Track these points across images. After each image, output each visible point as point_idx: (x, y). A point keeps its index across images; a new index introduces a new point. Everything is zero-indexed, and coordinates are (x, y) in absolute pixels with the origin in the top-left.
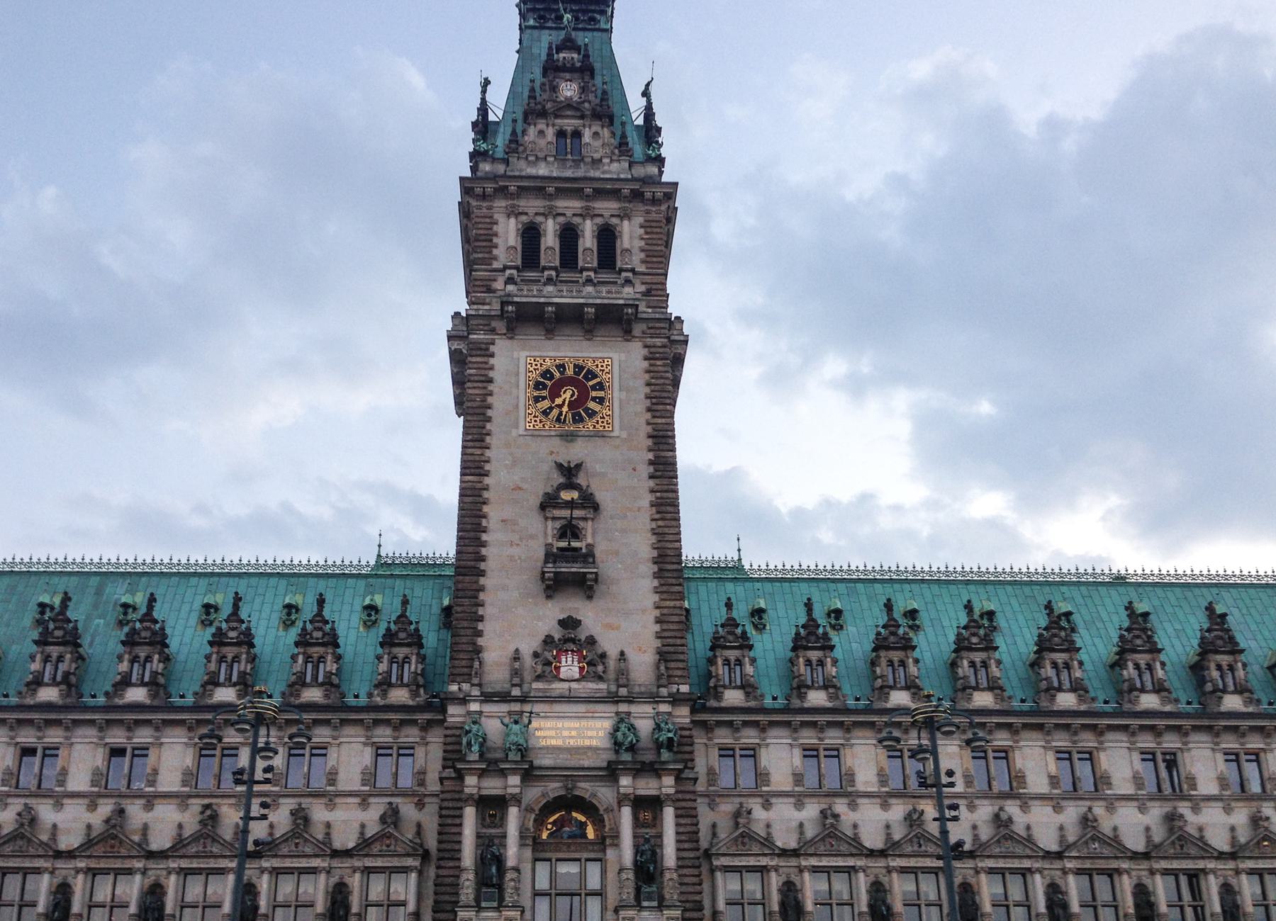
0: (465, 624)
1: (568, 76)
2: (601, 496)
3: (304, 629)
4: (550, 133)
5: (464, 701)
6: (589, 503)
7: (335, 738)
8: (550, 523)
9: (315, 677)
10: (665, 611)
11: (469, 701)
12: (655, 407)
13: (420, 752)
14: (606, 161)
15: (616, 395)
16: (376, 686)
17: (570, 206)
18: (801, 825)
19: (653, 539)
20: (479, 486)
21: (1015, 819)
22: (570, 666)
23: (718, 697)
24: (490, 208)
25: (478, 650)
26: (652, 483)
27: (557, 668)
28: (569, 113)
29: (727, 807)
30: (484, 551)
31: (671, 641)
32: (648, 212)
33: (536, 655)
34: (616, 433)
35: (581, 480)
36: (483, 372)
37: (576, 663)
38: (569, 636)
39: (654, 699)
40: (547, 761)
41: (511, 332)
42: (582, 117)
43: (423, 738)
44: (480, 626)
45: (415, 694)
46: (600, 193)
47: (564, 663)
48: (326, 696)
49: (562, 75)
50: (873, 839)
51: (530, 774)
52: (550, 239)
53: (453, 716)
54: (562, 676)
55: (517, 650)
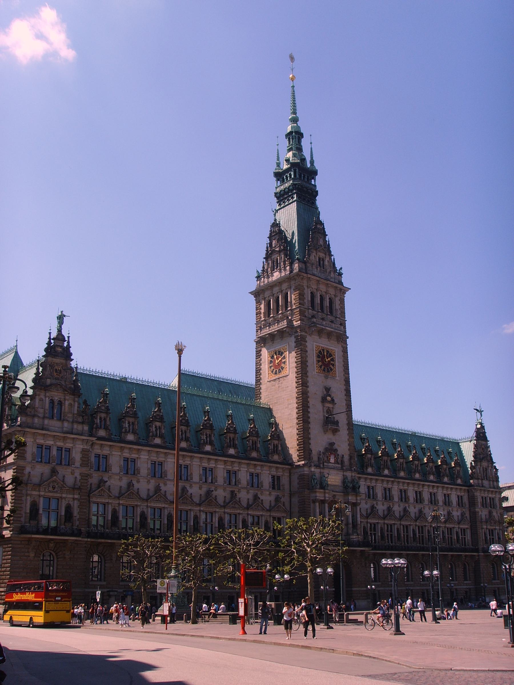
1: (320, 235)
2: (336, 401)
14: (332, 273)
15: (337, 364)
18: (367, 509)
26: (345, 397)
34: (337, 378)
41: (311, 335)
52: (318, 300)
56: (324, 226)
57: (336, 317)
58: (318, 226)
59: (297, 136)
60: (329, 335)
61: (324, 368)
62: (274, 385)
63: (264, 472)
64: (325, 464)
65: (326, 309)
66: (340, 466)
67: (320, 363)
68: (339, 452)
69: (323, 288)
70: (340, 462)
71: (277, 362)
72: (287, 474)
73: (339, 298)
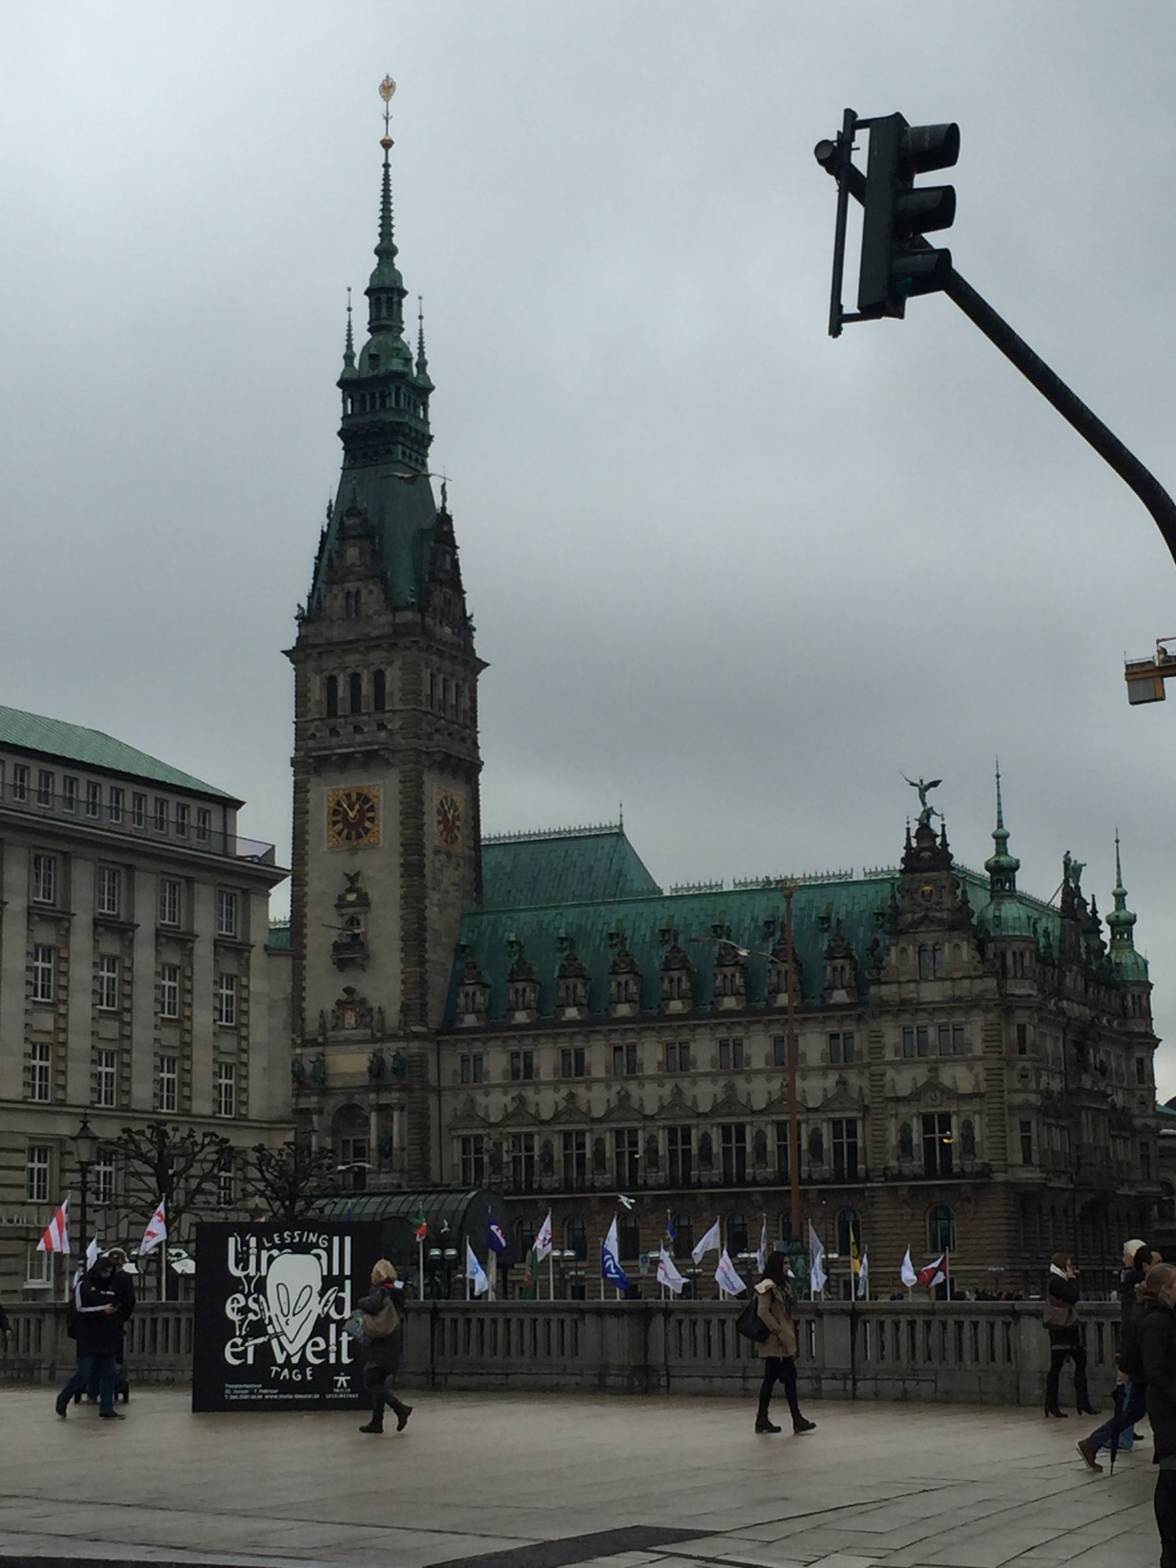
4: (341, 596)
6: (364, 901)
15: (381, 814)
17: (352, 659)
21: (633, 1093)
22: (350, 1018)
23: (462, 1021)
26: (401, 881)
28: (353, 577)
29: (463, 1096)
33: (333, 1011)
35: (358, 885)
38: (351, 1000)
39: (394, 1037)
40: (336, 1083)
44: (304, 994)
46: (369, 649)
50: (546, 1115)
51: (325, 1092)
52: (342, 691)
61: (349, 833)
65: (367, 704)
67: (339, 826)
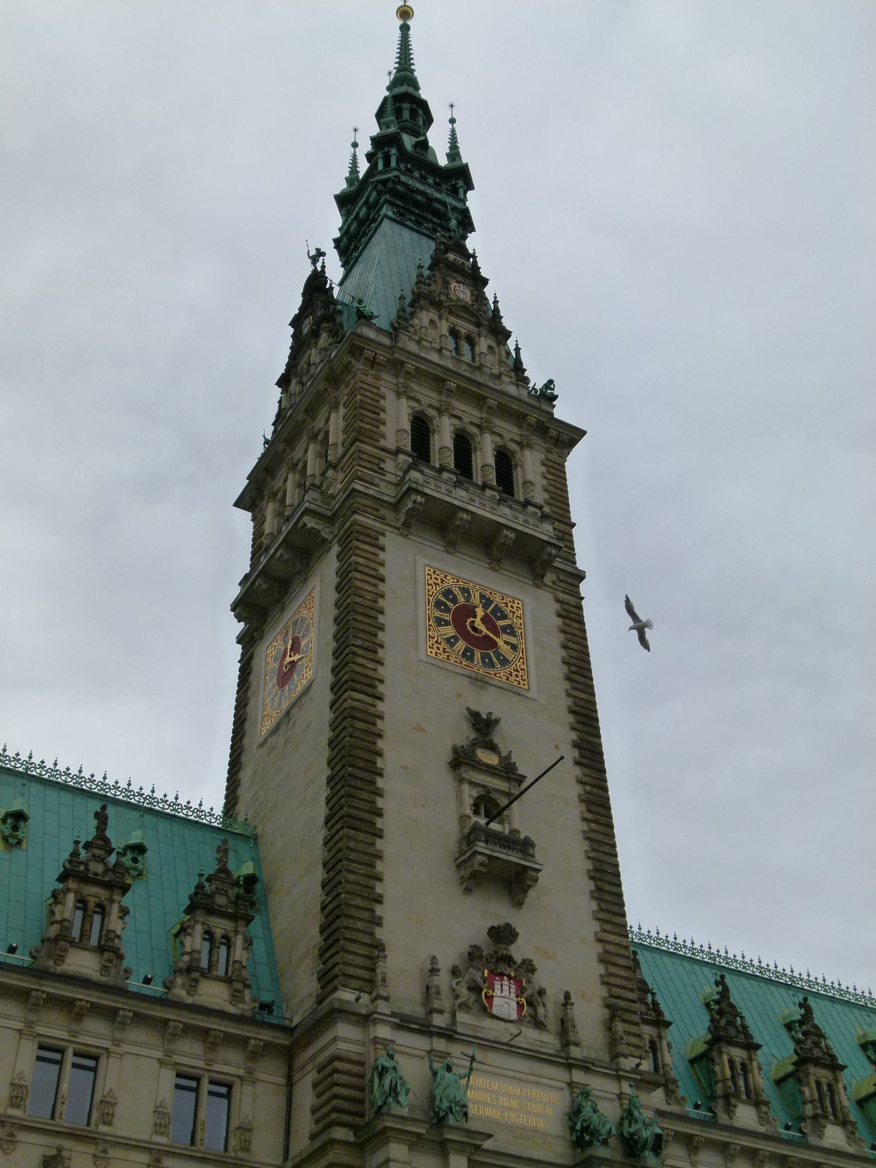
0: (359, 902)
1: (460, 278)
3: (75, 854)
4: (444, 327)
5: (365, 1020)
7: (117, 1042)
8: (466, 787)
9: (84, 933)
10: (610, 948)
11: (375, 1022)
12: (575, 677)
13: (243, 1094)
16: (177, 971)
19: (586, 846)
20: (372, 710)
24: (378, 378)
25: (380, 946)
27: (490, 998)
30: (380, 802)
31: (621, 992)
32: (549, 451)
33: (455, 972)
36: (373, 565)
37: (513, 995)
42: (478, 325)
43: (250, 1071)
44: (379, 910)
45: (236, 997)
47: (497, 992)
48: (104, 969)
49: (454, 274)
53: (346, 1040)
54: (495, 1011)
55: (434, 958)
56: (475, 262)
57: (527, 503)
58: (451, 256)
59: (406, 106)
60: (488, 542)
61: (467, 650)
62: (274, 748)
63: (126, 1048)
64: (461, 1017)
66: (548, 1041)
68: (541, 979)
69: (469, 413)
70: (552, 1024)
71: (288, 659)
72: (270, 1073)
73: (542, 457)
